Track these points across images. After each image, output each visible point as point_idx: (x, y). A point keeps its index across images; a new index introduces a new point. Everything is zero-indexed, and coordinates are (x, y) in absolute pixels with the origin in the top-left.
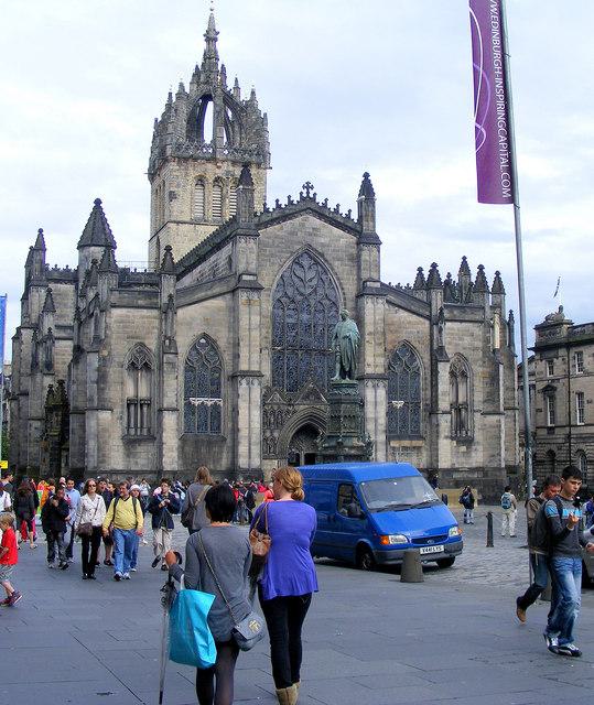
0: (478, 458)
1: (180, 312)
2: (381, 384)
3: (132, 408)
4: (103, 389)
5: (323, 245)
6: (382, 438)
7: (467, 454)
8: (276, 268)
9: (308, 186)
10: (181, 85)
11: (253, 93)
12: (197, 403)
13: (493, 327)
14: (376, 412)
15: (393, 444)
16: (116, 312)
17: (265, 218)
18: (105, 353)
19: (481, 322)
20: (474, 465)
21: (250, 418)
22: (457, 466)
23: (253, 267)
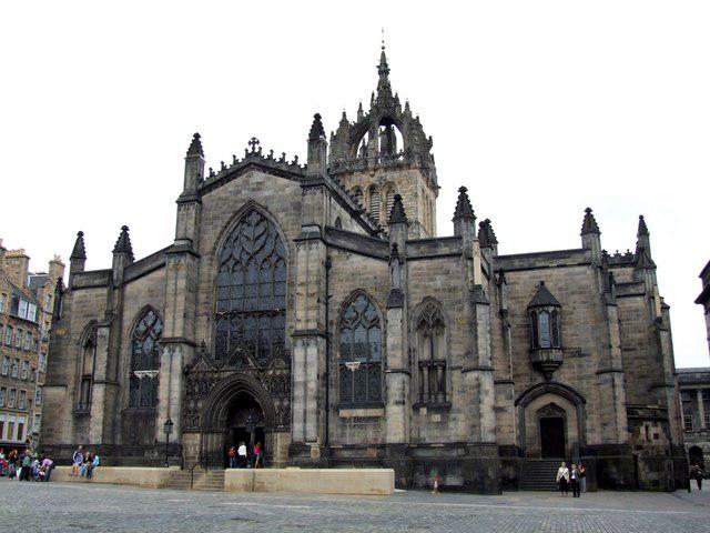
0: (458, 429)
1: (129, 288)
2: (312, 342)
3: (86, 384)
4: (56, 366)
5: (267, 198)
6: (312, 405)
7: (443, 424)
8: (219, 230)
9: (254, 142)
10: (344, 114)
11: (407, 105)
12: (139, 376)
13: (472, 259)
14: (306, 374)
15: (344, 413)
16: (77, 294)
17: (209, 183)
18: (61, 332)
19: (459, 255)
20: (453, 439)
21: (170, 387)
22: (428, 441)
23: (191, 236)
